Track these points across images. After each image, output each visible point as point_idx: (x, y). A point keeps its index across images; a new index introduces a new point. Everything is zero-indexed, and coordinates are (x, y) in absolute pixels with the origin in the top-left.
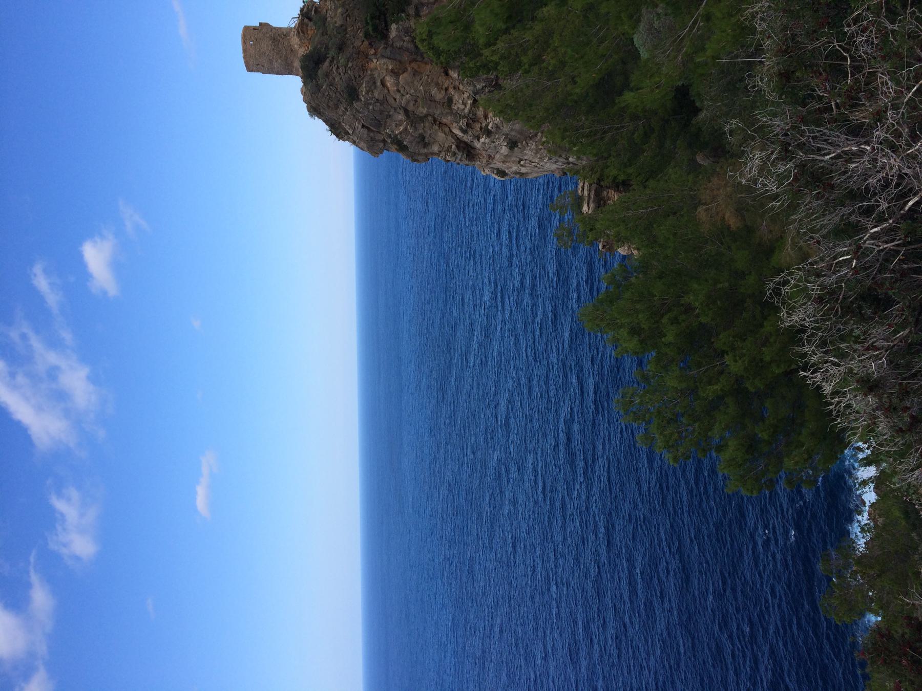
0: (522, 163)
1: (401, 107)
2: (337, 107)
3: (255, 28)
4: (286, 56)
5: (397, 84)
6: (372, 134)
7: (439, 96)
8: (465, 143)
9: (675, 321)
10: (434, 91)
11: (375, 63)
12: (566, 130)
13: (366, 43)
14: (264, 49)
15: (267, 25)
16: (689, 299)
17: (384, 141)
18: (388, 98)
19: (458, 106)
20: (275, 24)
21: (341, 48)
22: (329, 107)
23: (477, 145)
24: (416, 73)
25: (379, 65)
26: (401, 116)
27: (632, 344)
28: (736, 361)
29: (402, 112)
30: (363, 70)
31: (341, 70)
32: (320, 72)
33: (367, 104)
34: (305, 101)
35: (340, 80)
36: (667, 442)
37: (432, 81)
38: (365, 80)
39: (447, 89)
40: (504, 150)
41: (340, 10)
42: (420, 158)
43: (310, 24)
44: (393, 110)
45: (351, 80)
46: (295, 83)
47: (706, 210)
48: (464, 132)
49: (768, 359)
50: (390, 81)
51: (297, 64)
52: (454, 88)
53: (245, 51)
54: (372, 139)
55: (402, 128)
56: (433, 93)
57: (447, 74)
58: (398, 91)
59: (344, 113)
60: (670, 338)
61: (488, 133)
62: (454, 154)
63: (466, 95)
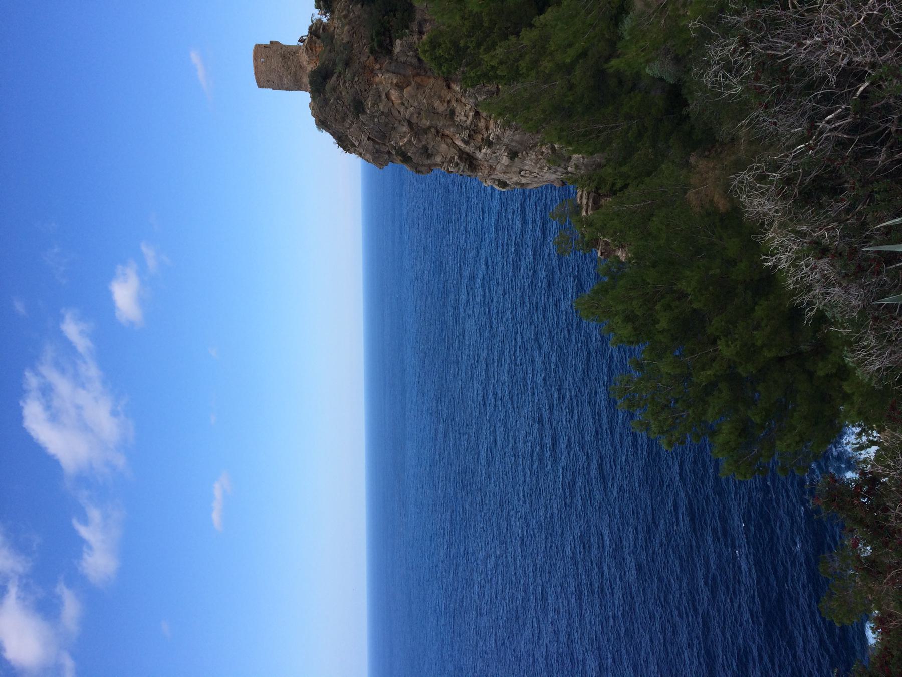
0: (522, 173)
1: (405, 119)
2: (344, 120)
3: (265, 46)
4: (295, 74)
5: (402, 97)
6: (377, 146)
7: (441, 108)
8: (467, 154)
9: (668, 308)
10: (437, 104)
11: (379, 77)
12: (562, 130)
13: (372, 58)
14: (275, 66)
15: (277, 43)
16: (682, 285)
17: (389, 153)
19: (460, 118)
20: (285, 41)
21: (347, 64)
22: (336, 120)
23: (479, 156)
24: (419, 86)
25: (384, 79)
26: (405, 129)
27: (626, 331)
28: (728, 346)
29: (406, 124)
31: (347, 85)
32: (328, 87)
33: (372, 117)
34: (313, 115)
35: (347, 95)
36: (662, 427)
38: (371, 93)
39: (449, 102)
40: (505, 161)
41: (346, 28)
42: (424, 169)
43: (319, 41)
44: (397, 122)
45: (357, 93)
46: (303, 99)
47: (697, 193)
48: (466, 143)
49: (759, 343)
50: (394, 95)
51: (306, 80)
52: (457, 101)
53: (256, 68)
54: (378, 151)
55: (406, 140)
56: (436, 105)
57: (449, 87)
58: (403, 104)
59: (351, 125)
60: (663, 324)
61: (490, 144)
62: (457, 165)
63: (468, 107)
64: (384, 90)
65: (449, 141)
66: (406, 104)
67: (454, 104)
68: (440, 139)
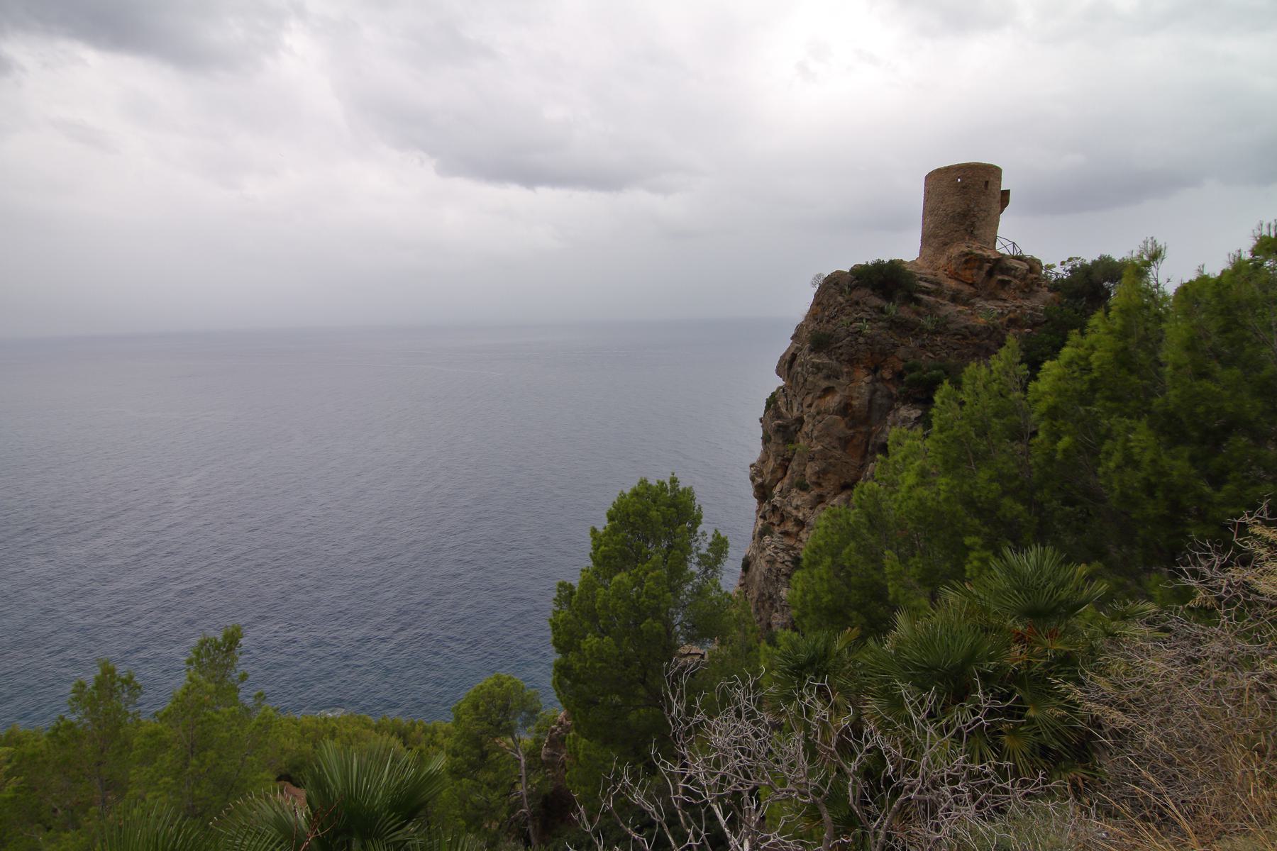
5: (827, 412)
11: (864, 379)
13: (900, 366)
18: (810, 396)
19: (798, 498)
24: (845, 442)
38: (835, 363)
39: (820, 485)
43: (983, 273)
50: (833, 401)
55: (784, 410)
65: (779, 474)
66: (818, 418)
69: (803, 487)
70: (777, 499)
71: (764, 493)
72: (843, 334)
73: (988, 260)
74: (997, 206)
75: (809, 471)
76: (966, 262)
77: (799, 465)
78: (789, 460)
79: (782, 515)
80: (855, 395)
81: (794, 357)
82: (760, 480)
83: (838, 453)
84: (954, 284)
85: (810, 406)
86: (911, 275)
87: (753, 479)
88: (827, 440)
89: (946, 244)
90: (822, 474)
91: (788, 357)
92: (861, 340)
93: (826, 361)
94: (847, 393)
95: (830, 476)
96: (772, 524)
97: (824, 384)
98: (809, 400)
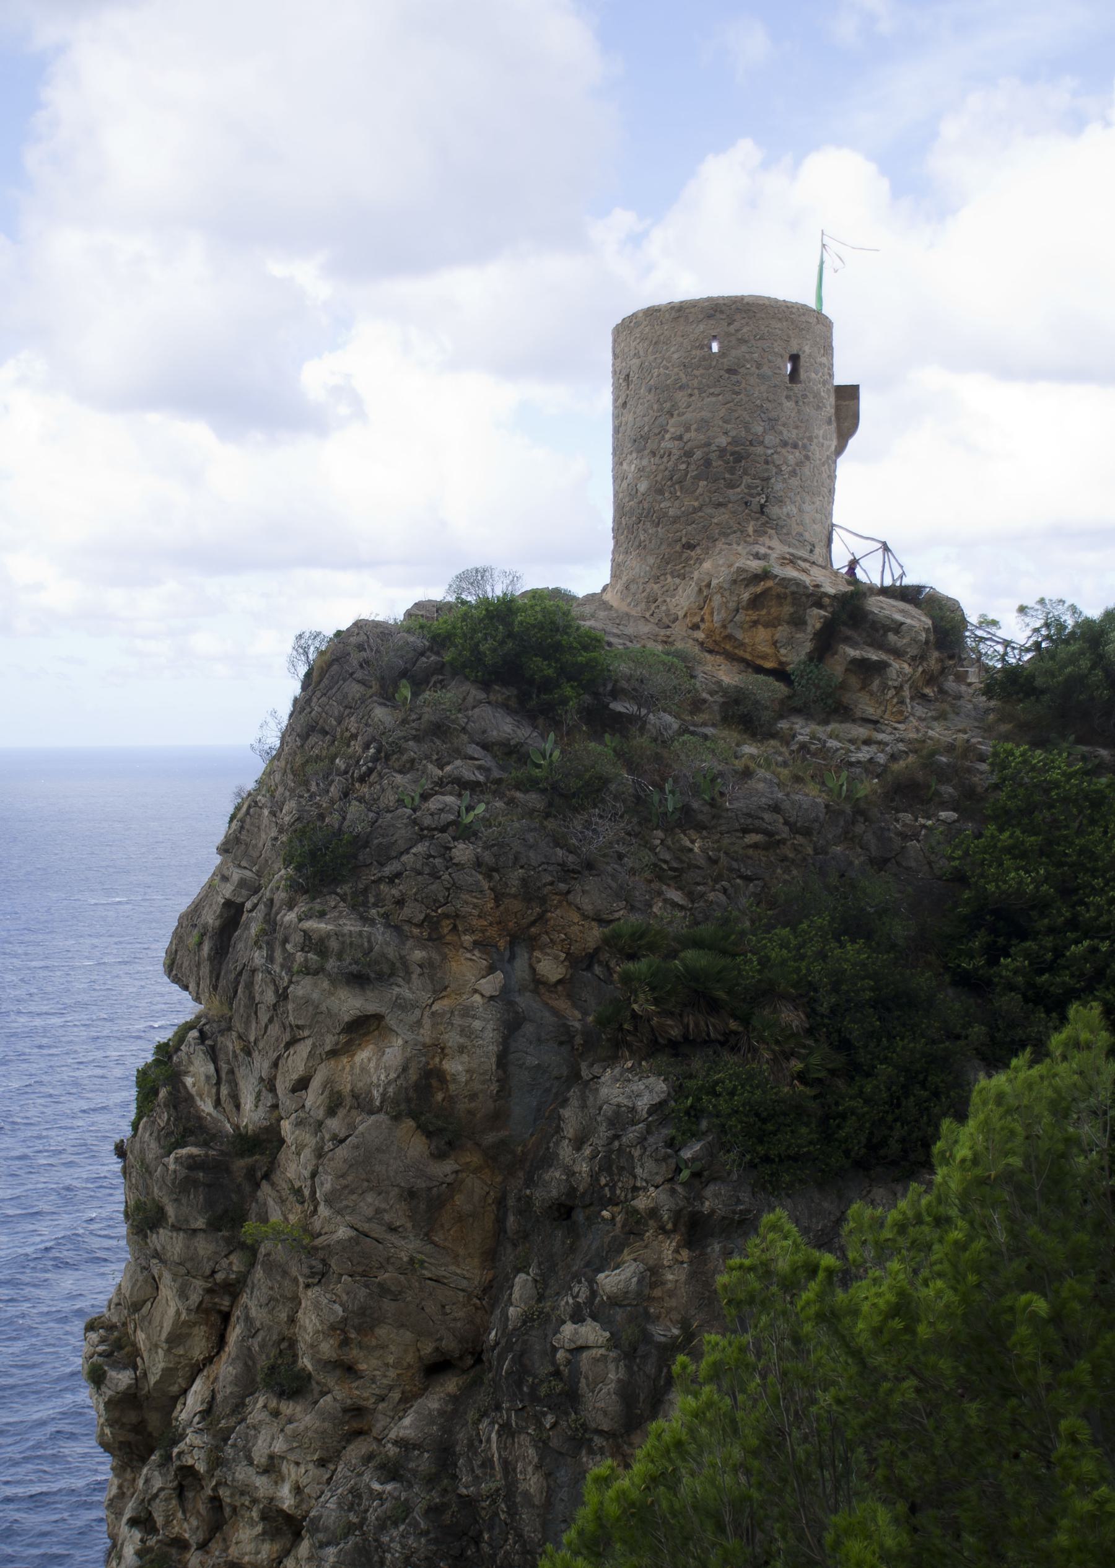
5: (362, 1103)
11: (474, 980)
14: (729, 408)
18: (303, 1050)
30: (431, 923)
37: (384, 1290)
38: (380, 935)
39: (349, 1370)
55: (206, 1106)
57: (436, 1368)
64: (400, 1005)
65: (198, 1348)
66: (334, 1124)
67: (338, 1394)
68: (195, 1298)
69: (292, 1385)
70: (193, 1449)
71: (139, 1428)
72: (402, 833)
73: (817, 598)
74: (825, 433)
75: (309, 1322)
76: (755, 602)
77: (271, 1303)
78: (233, 1289)
79: (216, 1502)
80: (452, 1039)
81: (232, 914)
82: (122, 1379)
83: (408, 1246)
84: (728, 676)
85: (302, 1084)
86: (592, 642)
87: (97, 1377)
88: (370, 1202)
89: (690, 546)
90: (353, 1328)
91: (210, 918)
92: (463, 852)
93: (351, 926)
94: (426, 1034)
95: (382, 1331)
96: (180, 1544)
97: (350, 1004)
98: (297, 1062)
